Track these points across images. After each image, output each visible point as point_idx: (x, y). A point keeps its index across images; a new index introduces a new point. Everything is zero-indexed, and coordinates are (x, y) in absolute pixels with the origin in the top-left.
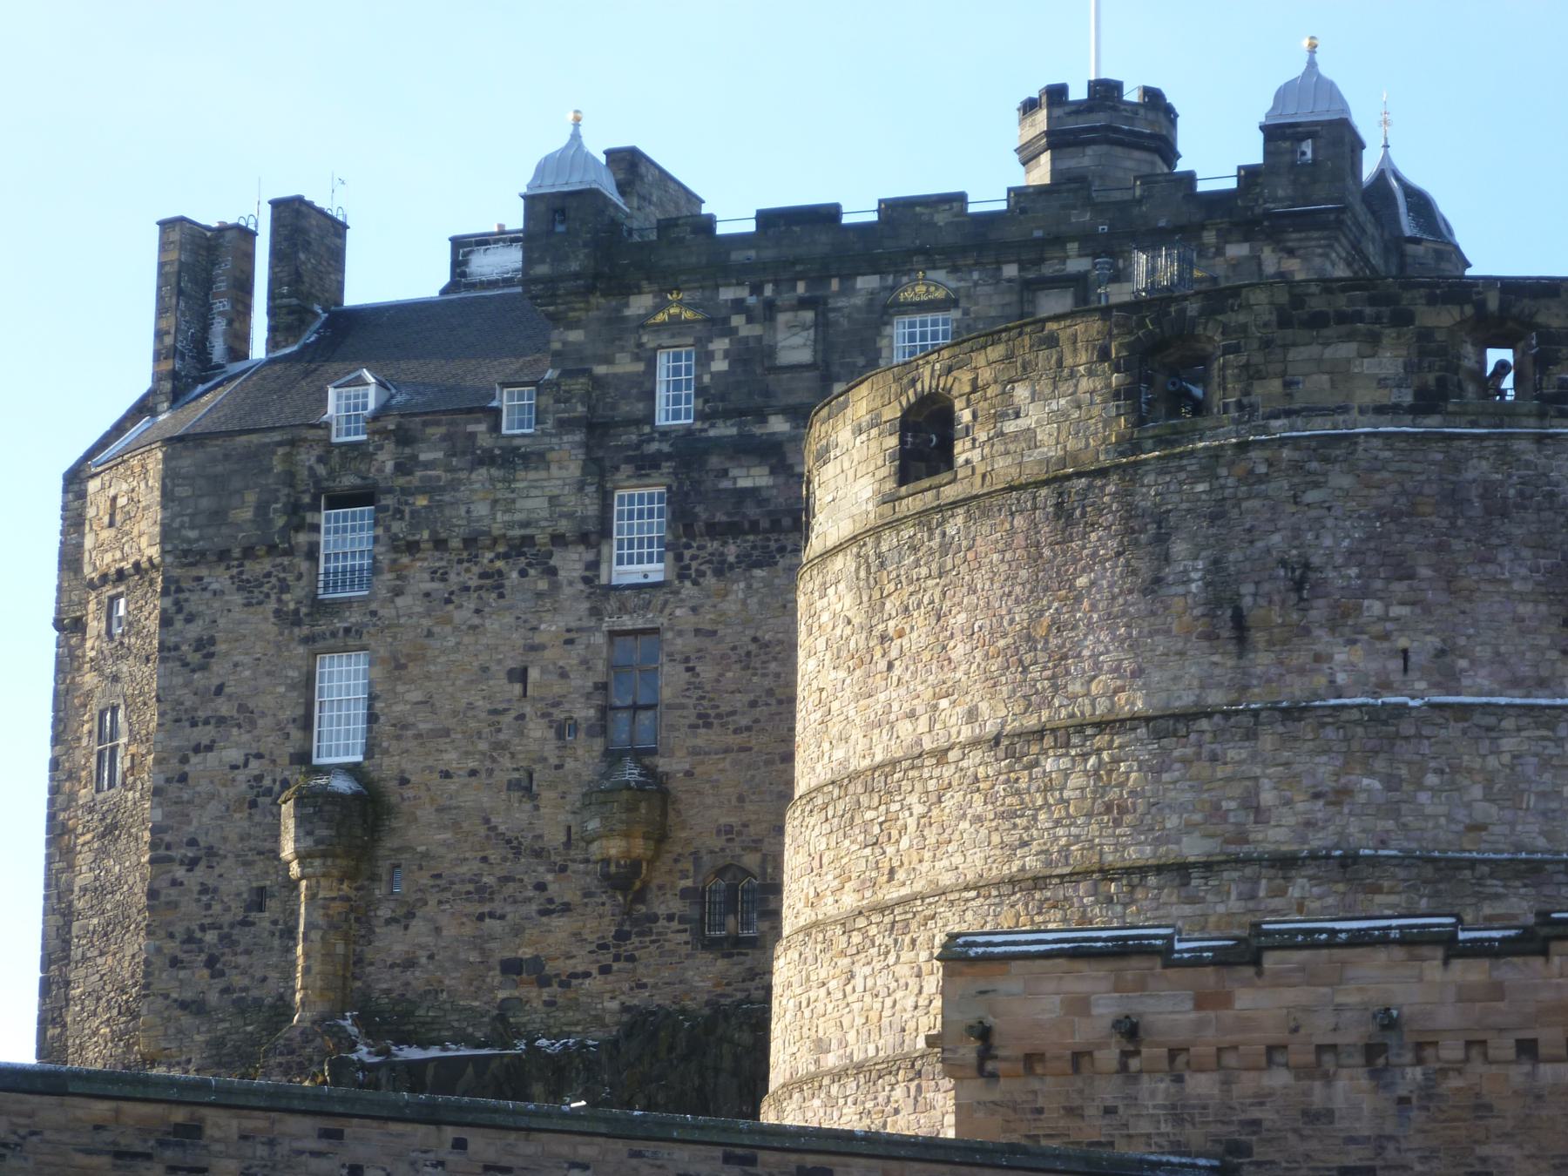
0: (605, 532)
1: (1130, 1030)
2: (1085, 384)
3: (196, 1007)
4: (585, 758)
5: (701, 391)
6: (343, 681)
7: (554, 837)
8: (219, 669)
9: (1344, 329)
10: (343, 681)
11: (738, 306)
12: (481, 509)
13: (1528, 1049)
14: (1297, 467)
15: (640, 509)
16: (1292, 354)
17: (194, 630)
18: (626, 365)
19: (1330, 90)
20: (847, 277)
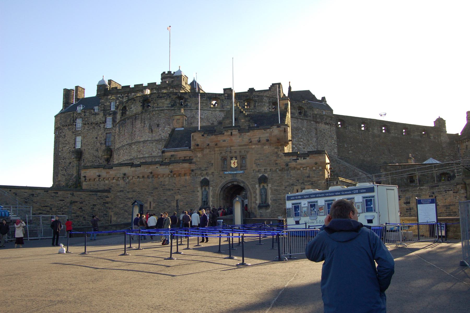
0: (105, 122)
1: (99, 176)
3: (64, 175)
4: (103, 147)
5: (116, 106)
6: (79, 139)
7: (100, 156)
8: (66, 138)
10: (79, 139)
11: (120, 97)
12: (93, 120)
13: (138, 177)
14: (158, 113)
15: (109, 119)
17: (64, 134)
18: (108, 104)
19: (181, 72)
20: (131, 93)
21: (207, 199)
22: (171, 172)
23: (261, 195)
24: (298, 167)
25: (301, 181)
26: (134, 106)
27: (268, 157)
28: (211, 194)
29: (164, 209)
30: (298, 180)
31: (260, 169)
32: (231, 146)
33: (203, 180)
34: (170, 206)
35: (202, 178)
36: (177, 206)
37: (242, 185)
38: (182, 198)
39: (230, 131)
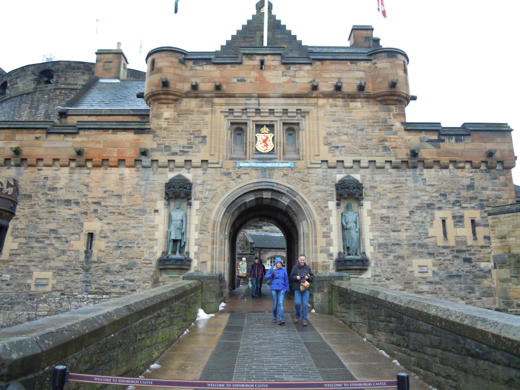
2: (30, 78)
9: (78, 70)
14: (65, 94)
16: (67, 74)
21: (183, 234)
22: (79, 153)
23: (344, 229)
24: (444, 160)
25: (452, 198)
26: (21, 81)
27: (362, 130)
28: (195, 219)
29: (47, 259)
30: (444, 195)
31: (340, 159)
32: (260, 96)
33: (172, 181)
34: (64, 252)
35: (171, 175)
36: (88, 253)
37: (285, 201)
38: (106, 227)
39: (258, 58)
